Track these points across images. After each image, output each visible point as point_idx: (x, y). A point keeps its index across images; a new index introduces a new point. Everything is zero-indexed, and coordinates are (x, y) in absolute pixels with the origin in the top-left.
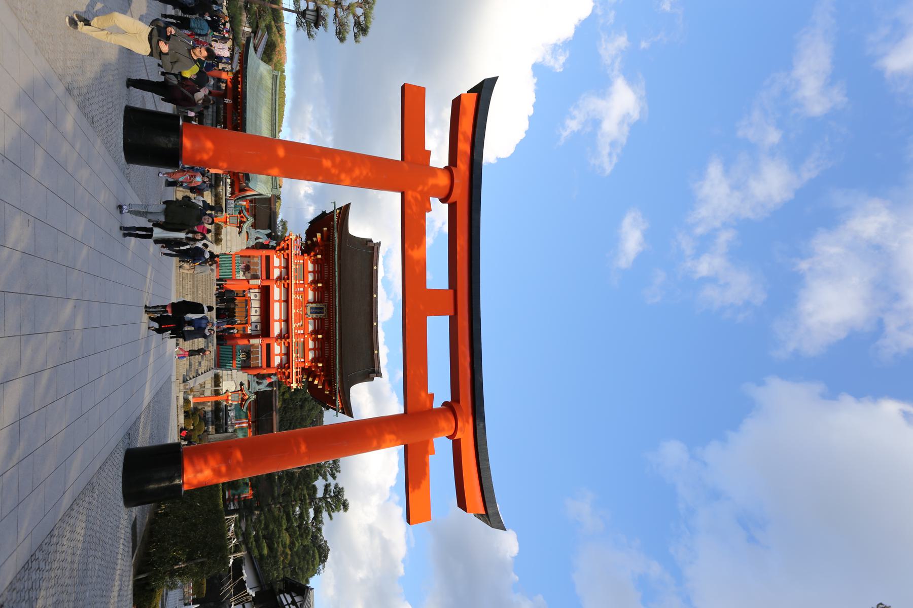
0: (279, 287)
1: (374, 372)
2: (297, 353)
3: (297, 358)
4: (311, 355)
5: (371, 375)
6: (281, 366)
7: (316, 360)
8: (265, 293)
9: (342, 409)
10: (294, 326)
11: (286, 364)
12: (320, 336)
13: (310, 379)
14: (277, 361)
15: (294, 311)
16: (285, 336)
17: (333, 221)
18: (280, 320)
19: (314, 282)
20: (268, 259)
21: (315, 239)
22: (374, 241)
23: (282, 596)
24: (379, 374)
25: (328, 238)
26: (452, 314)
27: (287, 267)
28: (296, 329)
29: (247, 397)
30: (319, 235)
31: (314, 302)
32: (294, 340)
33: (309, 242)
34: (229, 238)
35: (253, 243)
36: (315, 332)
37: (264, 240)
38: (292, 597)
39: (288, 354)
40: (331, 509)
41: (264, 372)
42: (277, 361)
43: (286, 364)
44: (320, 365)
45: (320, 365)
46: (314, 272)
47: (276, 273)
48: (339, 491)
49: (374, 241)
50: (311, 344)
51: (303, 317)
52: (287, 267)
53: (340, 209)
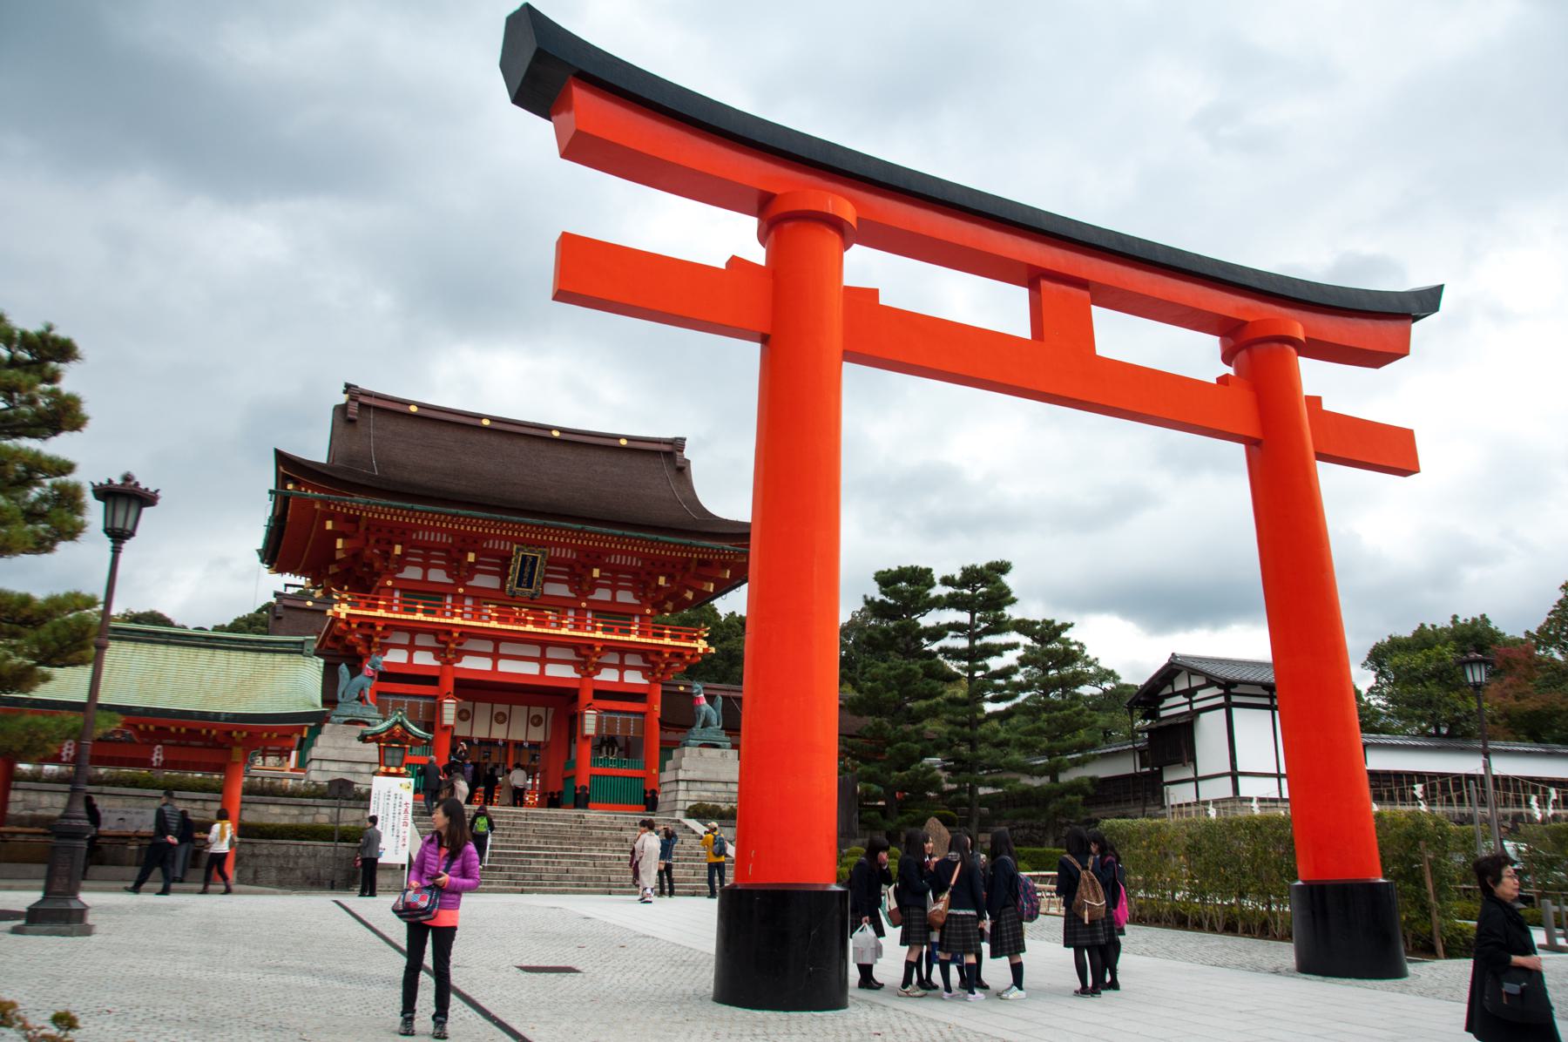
0: (460, 654)
4: (625, 597)
6: (645, 672)
8: (473, 690)
11: (650, 659)
15: (530, 628)
17: (312, 502)
18: (543, 661)
20: (388, 676)
21: (339, 555)
22: (343, 399)
23: (1163, 714)
24: (678, 444)
25: (350, 524)
26: (1086, 294)
27: (414, 629)
31: (504, 576)
38: (1175, 694)
39: (623, 650)
40: (1002, 598)
41: (657, 708)
42: (634, 678)
43: (650, 659)
44: (662, 581)
45: (662, 581)
46: (426, 567)
47: (424, 659)
48: (972, 576)
49: (343, 399)
51: (539, 606)
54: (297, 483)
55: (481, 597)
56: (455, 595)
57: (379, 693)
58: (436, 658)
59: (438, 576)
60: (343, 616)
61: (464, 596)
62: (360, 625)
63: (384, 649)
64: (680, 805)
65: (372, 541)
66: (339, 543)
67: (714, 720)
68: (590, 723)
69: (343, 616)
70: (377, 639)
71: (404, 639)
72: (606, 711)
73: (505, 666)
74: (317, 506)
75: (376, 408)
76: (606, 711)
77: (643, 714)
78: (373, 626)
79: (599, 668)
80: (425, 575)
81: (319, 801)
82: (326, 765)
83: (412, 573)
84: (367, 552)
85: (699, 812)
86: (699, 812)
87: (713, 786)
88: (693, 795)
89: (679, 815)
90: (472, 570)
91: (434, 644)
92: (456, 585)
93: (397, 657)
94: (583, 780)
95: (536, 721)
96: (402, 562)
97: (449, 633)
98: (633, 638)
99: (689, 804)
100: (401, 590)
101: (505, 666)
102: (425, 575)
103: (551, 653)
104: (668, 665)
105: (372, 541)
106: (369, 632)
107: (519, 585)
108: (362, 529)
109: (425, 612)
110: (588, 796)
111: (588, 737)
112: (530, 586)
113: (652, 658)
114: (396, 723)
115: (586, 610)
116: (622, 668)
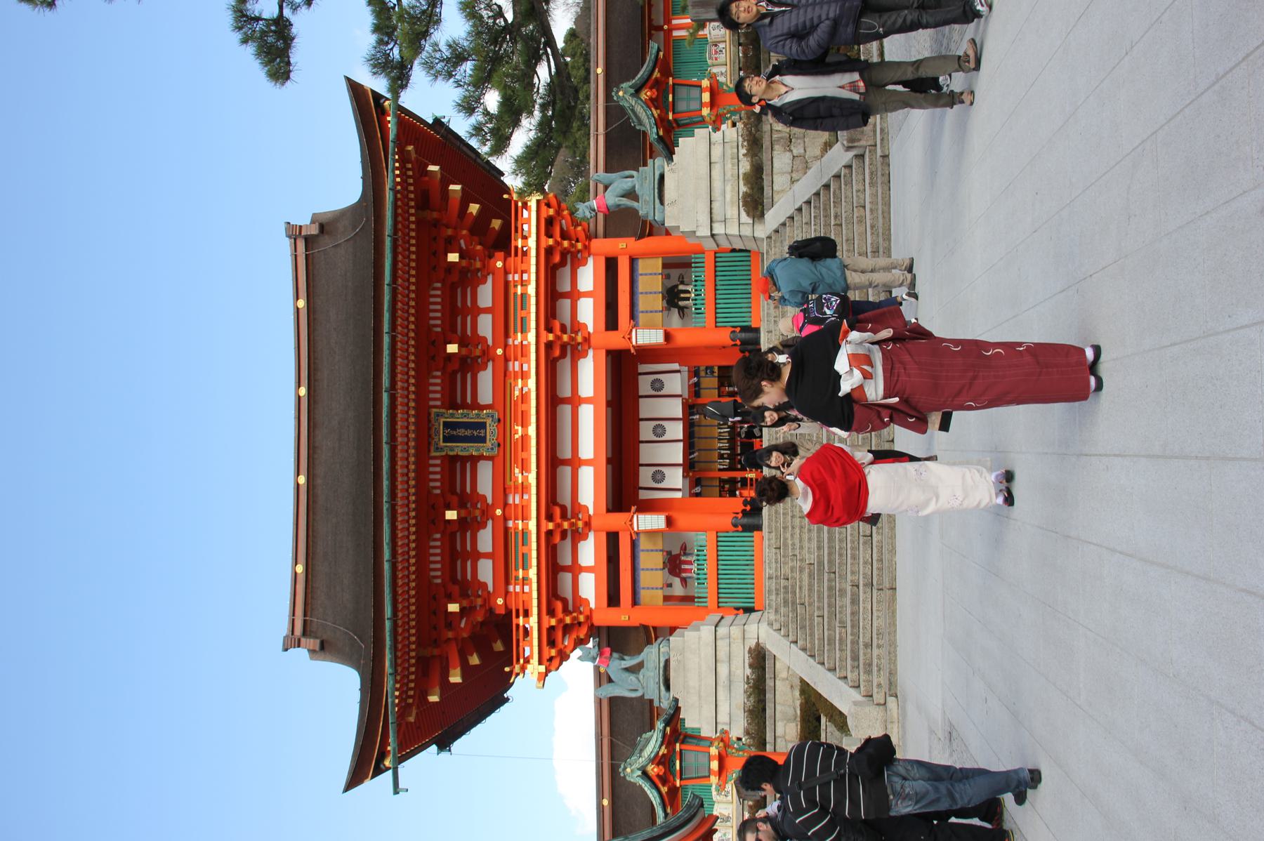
0: (577, 508)
1: (309, 240)
2: (524, 296)
3: (524, 284)
4: (485, 295)
5: (314, 230)
6: (578, 262)
7: (467, 278)
9: (382, 112)
10: (532, 383)
12: (452, 348)
13: (496, 224)
14: (588, 277)
16: (560, 351)
19: (469, 525)
21: (475, 660)
22: (301, 654)
24: (294, 233)
27: (553, 569)
28: (524, 375)
29: (646, 94)
30: (456, 678)
31: (475, 460)
32: (531, 337)
33: (499, 646)
34: (723, 670)
35: (651, 655)
36: (468, 365)
37: (616, 666)
39: (552, 296)
42: (588, 277)
43: (557, 263)
44: (453, 257)
45: (453, 257)
46: (477, 556)
47: (589, 552)
50: (485, 326)
51: (506, 408)
52: (555, 569)
53: (378, 771)
54: (383, 755)
55: (503, 486)
56: (505, 518)
57: (635, 602)
58: (585, 537)
59: (485, 540)
60: (542, 669)
61: (505, 506)
62: (552, 643)
63: (579, 601)
64: (747, 231)
65: (450, 635)
66: (456, 678)
67: (626, 184)
68: (648, 337)
69: (542, 669)
70: (568, 620)
71: (567, 578)
72: (633, 316)
73: (587, 448)
74: (412, 719)
75: (305, 615)
76: (633, 316)
77: (633, 261)
78: (551, 629)
79: (577, 327)
80: (486, 556)
81: (769, 738)
82: (723, 717)
83: (486, 571)
84: (465, 635)
85: (755, 203)
86: (755, 203)
87: (717, 184)
88: (732, 212)
89: (762, 231)
90: (467, 500)
91: (568, 542)
92: (494, 517)
93: (589, 588)
94: (724, 337)
95: (657, 385)
96: (467, 589)
97: (549, 533)
98: (531, 290)
99: (745, 218)
100: (507, 583)
101: (587, 448)
102: (486, 556)
103: (566, 392)
104: (564, 235)
105: (450, 635)
106: (560, 634)
107: (483, 440)
108: (435, 652)
109: (525, 568)
110: (745, 329)
111: (668, 336)
112: (482, 426)
113: (557, 259)
114: (645, 774)
115: (506, 347)
116: (574, 295)
